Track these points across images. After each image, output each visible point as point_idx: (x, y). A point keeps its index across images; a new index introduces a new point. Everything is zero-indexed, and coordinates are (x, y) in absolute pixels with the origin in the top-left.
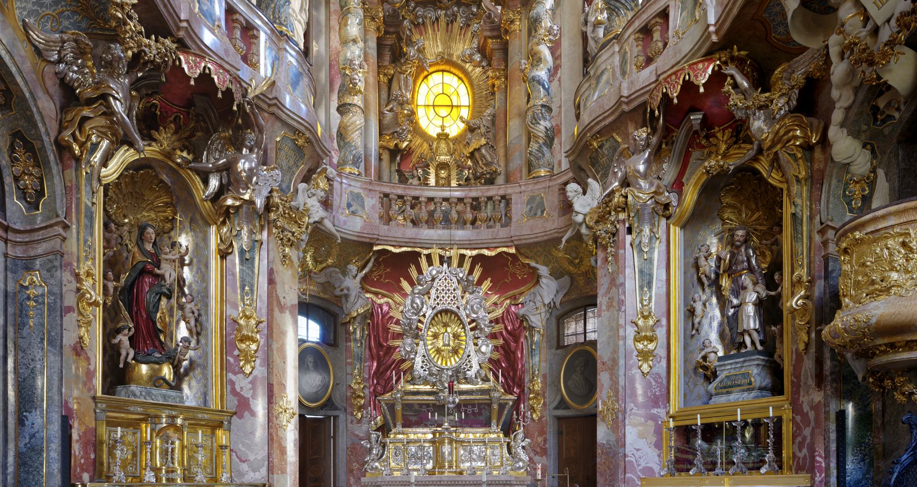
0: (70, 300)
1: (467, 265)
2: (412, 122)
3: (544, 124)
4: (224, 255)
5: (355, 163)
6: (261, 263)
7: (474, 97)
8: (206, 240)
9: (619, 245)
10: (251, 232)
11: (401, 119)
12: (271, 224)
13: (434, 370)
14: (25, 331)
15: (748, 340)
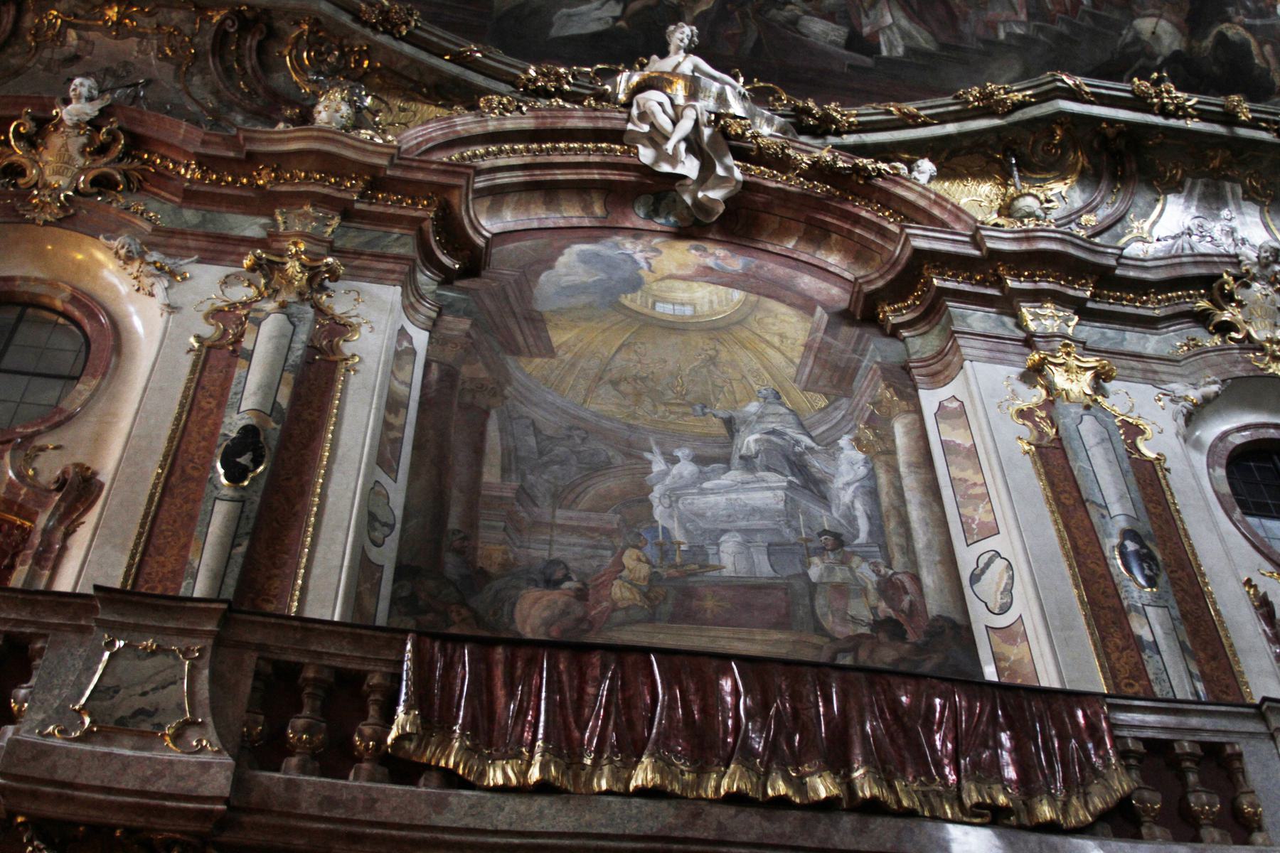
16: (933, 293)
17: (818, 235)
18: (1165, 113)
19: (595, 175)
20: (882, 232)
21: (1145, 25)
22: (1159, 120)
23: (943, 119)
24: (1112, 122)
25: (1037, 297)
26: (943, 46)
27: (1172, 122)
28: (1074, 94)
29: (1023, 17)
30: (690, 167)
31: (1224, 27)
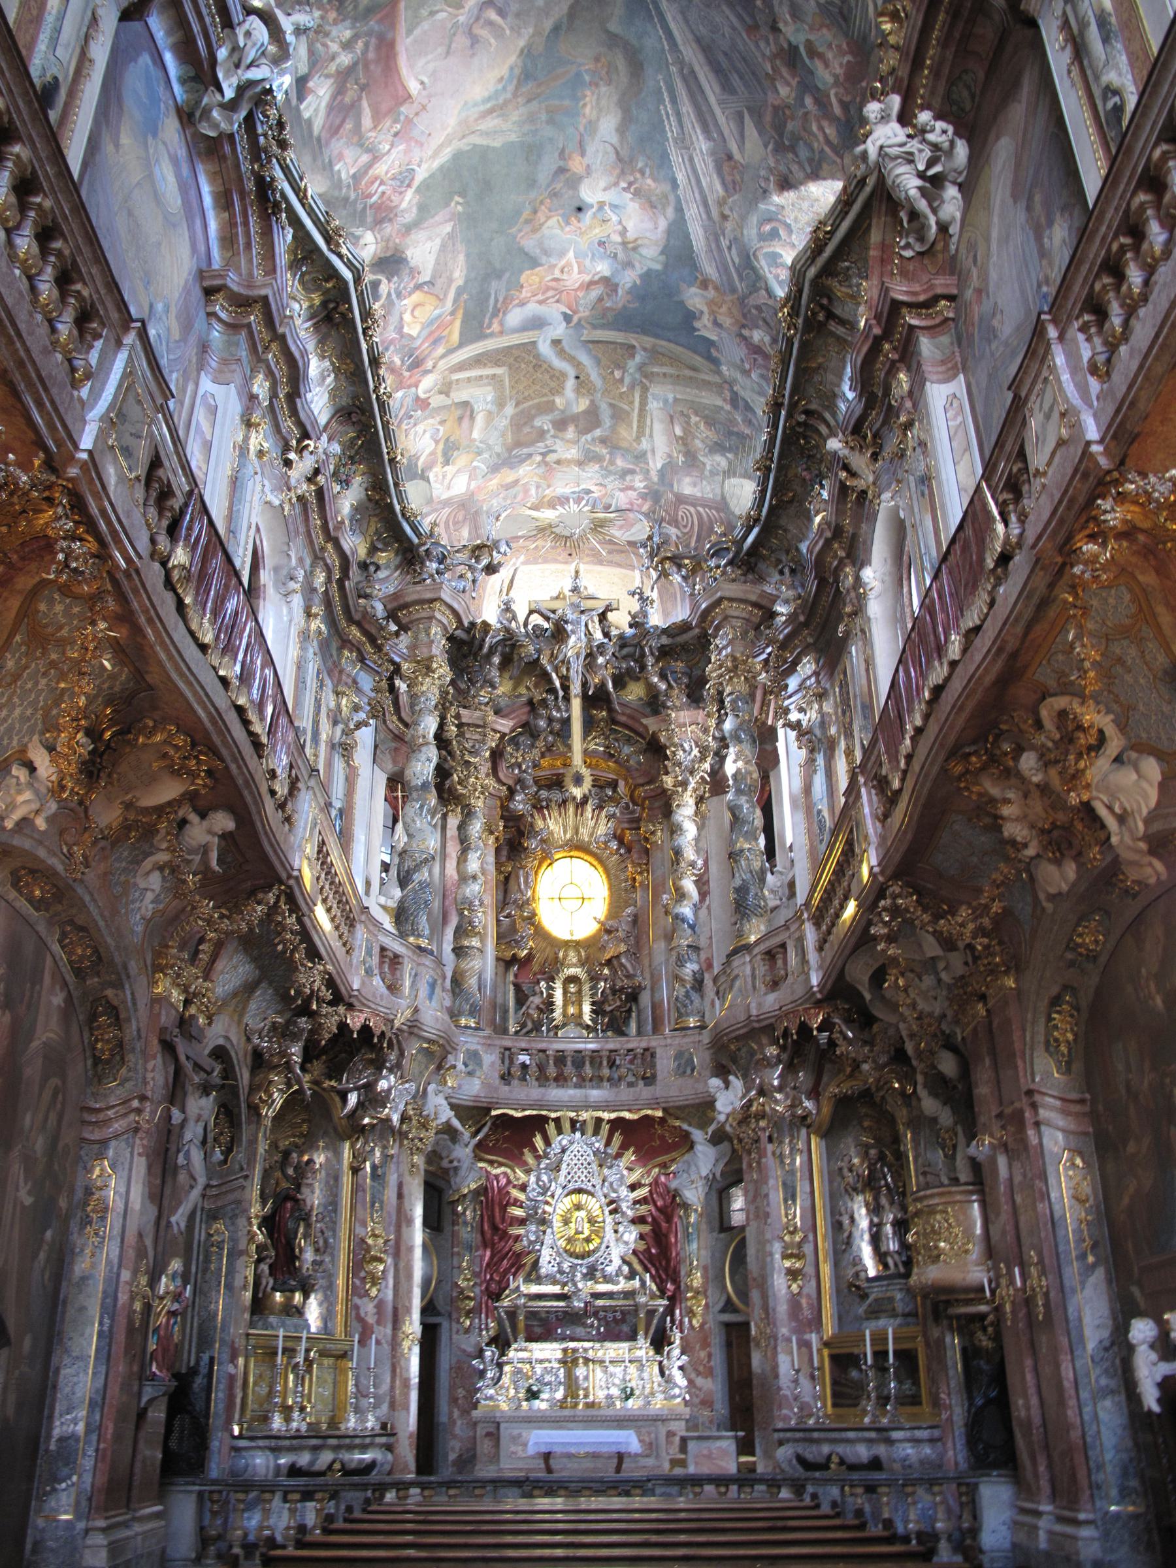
0: (242, 1245)
1: (606, 1128)
2: (532, 924)
3: (690, 968)
4: (356, 1170)
5: (472, 1013)
6: (392, 1179)
7: (611, 888)
8: (338, 1154)
9: (762, 1154)
10: (384, 1147)
11: (519, 924)
12: (403, 1135)
13: (566, 1266)
14: (208, 1275)
15: (890, 1261)
16: (246, 321)
17: (224, 201)
18: (365, 331)
19: (196, 28)
20: (248, 245)
21: (369, 237)
22: (360, 331)
23: (311, 213)
24: (351, 309)
25: (270, 374)
26: (319, 139)
27: (361, 337)
28: (358, 280)
29: (352, 171)
30: (229, 94)
31: (385, 281)
